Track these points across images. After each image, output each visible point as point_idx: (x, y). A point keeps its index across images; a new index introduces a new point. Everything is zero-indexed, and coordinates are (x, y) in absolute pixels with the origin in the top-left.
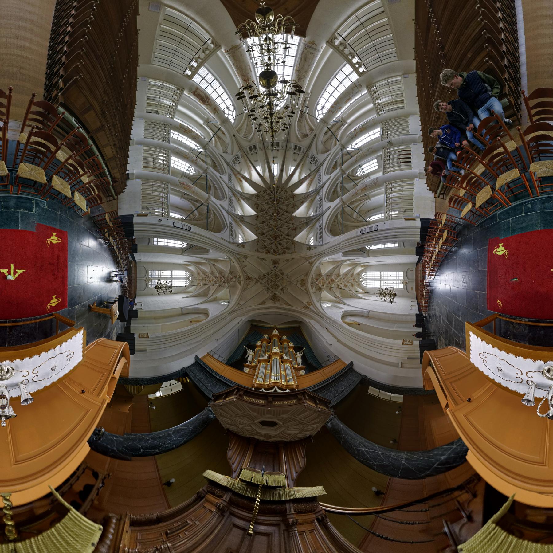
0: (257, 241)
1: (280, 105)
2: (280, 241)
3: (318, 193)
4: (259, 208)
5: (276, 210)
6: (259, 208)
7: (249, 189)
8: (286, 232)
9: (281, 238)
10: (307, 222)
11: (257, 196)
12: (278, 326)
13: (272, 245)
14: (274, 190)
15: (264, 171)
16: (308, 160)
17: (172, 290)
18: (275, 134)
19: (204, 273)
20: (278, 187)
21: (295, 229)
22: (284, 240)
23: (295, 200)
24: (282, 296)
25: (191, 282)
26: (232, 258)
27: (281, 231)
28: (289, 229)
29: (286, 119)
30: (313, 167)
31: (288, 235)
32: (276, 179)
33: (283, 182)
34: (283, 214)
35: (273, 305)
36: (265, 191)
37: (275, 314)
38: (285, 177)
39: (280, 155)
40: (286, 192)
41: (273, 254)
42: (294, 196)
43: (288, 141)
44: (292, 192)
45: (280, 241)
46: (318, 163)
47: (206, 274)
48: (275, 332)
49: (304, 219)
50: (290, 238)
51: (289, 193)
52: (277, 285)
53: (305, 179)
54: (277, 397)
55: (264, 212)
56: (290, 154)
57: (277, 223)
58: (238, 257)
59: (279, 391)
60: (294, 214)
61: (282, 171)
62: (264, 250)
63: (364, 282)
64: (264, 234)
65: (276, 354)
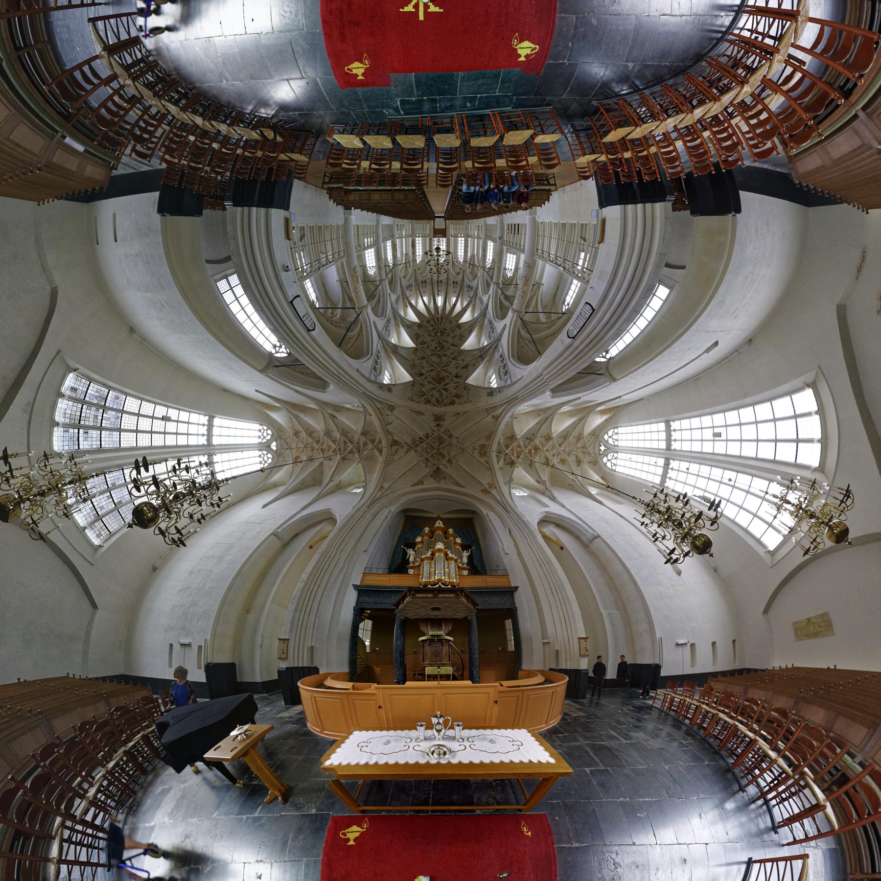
0: (412, 384)
1: (442, 260)
2: (445, 385)
3: (485, 315)
4: (420, 340)
5: (439, 343)
6: (420, 340)
7: (412, 317)
8: (454, 373)
9: (447, 381)
10: (481, 354)
11: (419, 325)
12: (442, 516)
13: (434, 392)
14: (438, 320)
15: (429, 302)
16: (465, 289)
17: (221, 493)
18: (440, 275)
19: (310, 433)
20: (442, 318)
21: (466, 367)
22: (452, 384)
23: (462, 330)
24: (449, 471)
25: (277, 454)
26: (368, 407)
27: (446, 371)
28: (457, 367)
29: (445, 267)
30: (471, 294)
31: (457, 377)
32: (440, 309)
33: (447, 312)
34: (449, 349)
35: (436, 485)
36: (428, 322)
37: (440, 498)
38: (448, 308)
39: (443, 289)
40: (451, 322)
41: (435, 405)
42: (459, 326)
43: (448, 279)
44: (457, 322)
45: (445, 385)
46: (474, 289)
47: (314, 435)
48: (439, 524)
49: (477, 352)
50: (459, 380)
51: (454, 323)
52: (441, 454)
53: (468, 306)
54: (440, 590)
55: (425, 346)
56: (451, 288)
57: (441, 360)
58: (379, 406)
59: (443, 586)
60: (462, 348)
61: (445, 302)
62: (422, 399)
63: (610, 457)
64: (422, 375)
65: (440, 550)
